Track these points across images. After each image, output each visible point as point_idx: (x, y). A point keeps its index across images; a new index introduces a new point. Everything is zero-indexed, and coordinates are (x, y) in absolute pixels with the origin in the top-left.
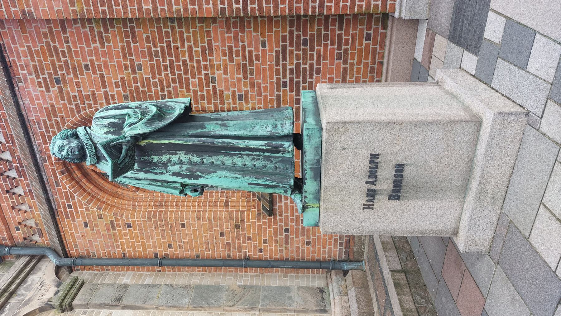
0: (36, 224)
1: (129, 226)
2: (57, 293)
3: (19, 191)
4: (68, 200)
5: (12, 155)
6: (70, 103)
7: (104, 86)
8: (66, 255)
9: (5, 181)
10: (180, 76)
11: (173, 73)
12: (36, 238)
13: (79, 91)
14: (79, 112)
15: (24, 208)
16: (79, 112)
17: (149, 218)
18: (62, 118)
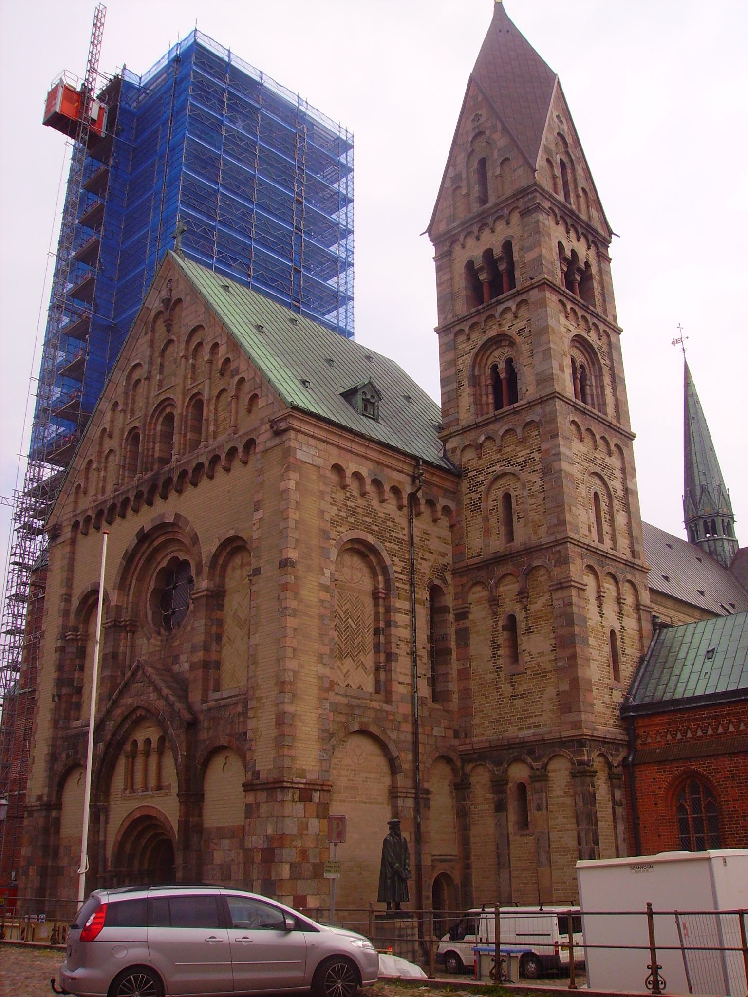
0: (649, 743)
1: (656, 804)
2: (616, 767)
3: (669, 737)
4: (668, 771)
5: (690, 738)
6: (723, 781)
7: (733, 800)
8: (634, 765)
9: (674, 731)
10: (743, 840)
11: (744, 837)
12: (639, 742)
13: (729, 787)
14: (719, 785)
15: (658, 737)
16: (719, 785)
17: (662, 816)
18: (714, 776)
